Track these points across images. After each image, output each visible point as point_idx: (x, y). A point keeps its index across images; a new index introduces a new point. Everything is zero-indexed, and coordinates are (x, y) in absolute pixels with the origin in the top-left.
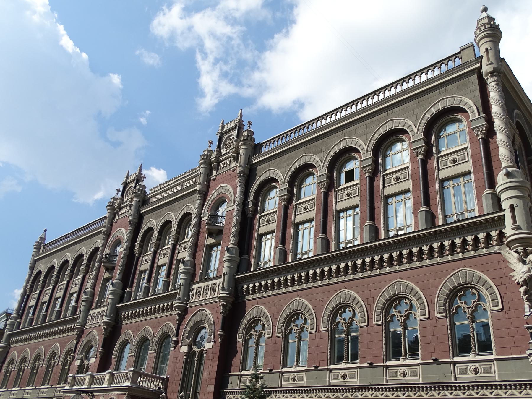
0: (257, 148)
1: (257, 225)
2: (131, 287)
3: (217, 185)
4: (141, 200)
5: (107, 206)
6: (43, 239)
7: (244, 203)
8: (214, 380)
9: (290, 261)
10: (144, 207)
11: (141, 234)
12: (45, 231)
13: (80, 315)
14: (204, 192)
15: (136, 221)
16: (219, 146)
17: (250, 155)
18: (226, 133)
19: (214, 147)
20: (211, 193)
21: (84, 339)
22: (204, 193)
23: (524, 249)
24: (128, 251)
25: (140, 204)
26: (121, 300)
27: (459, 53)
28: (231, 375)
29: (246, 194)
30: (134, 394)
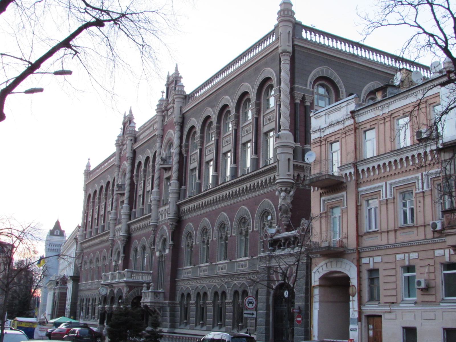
0: (186, 98)
2: (135, 208)
4: (133, 139)
6: (88, 166)
7: (180, 146)
8: (170, 274)
9: (229, 179)
11: (136, 167)
12: (89, 159)
13: (111, 231)
16: (167, 96)
17: (181, 107)
18: (170, 84)
19: (165, 97)
21: (115, 248)
23: (281, 188)
25: (133, 142)
26: (130, 220)
27: (274, 30)
29: (181, 138)
30: (130, 285)
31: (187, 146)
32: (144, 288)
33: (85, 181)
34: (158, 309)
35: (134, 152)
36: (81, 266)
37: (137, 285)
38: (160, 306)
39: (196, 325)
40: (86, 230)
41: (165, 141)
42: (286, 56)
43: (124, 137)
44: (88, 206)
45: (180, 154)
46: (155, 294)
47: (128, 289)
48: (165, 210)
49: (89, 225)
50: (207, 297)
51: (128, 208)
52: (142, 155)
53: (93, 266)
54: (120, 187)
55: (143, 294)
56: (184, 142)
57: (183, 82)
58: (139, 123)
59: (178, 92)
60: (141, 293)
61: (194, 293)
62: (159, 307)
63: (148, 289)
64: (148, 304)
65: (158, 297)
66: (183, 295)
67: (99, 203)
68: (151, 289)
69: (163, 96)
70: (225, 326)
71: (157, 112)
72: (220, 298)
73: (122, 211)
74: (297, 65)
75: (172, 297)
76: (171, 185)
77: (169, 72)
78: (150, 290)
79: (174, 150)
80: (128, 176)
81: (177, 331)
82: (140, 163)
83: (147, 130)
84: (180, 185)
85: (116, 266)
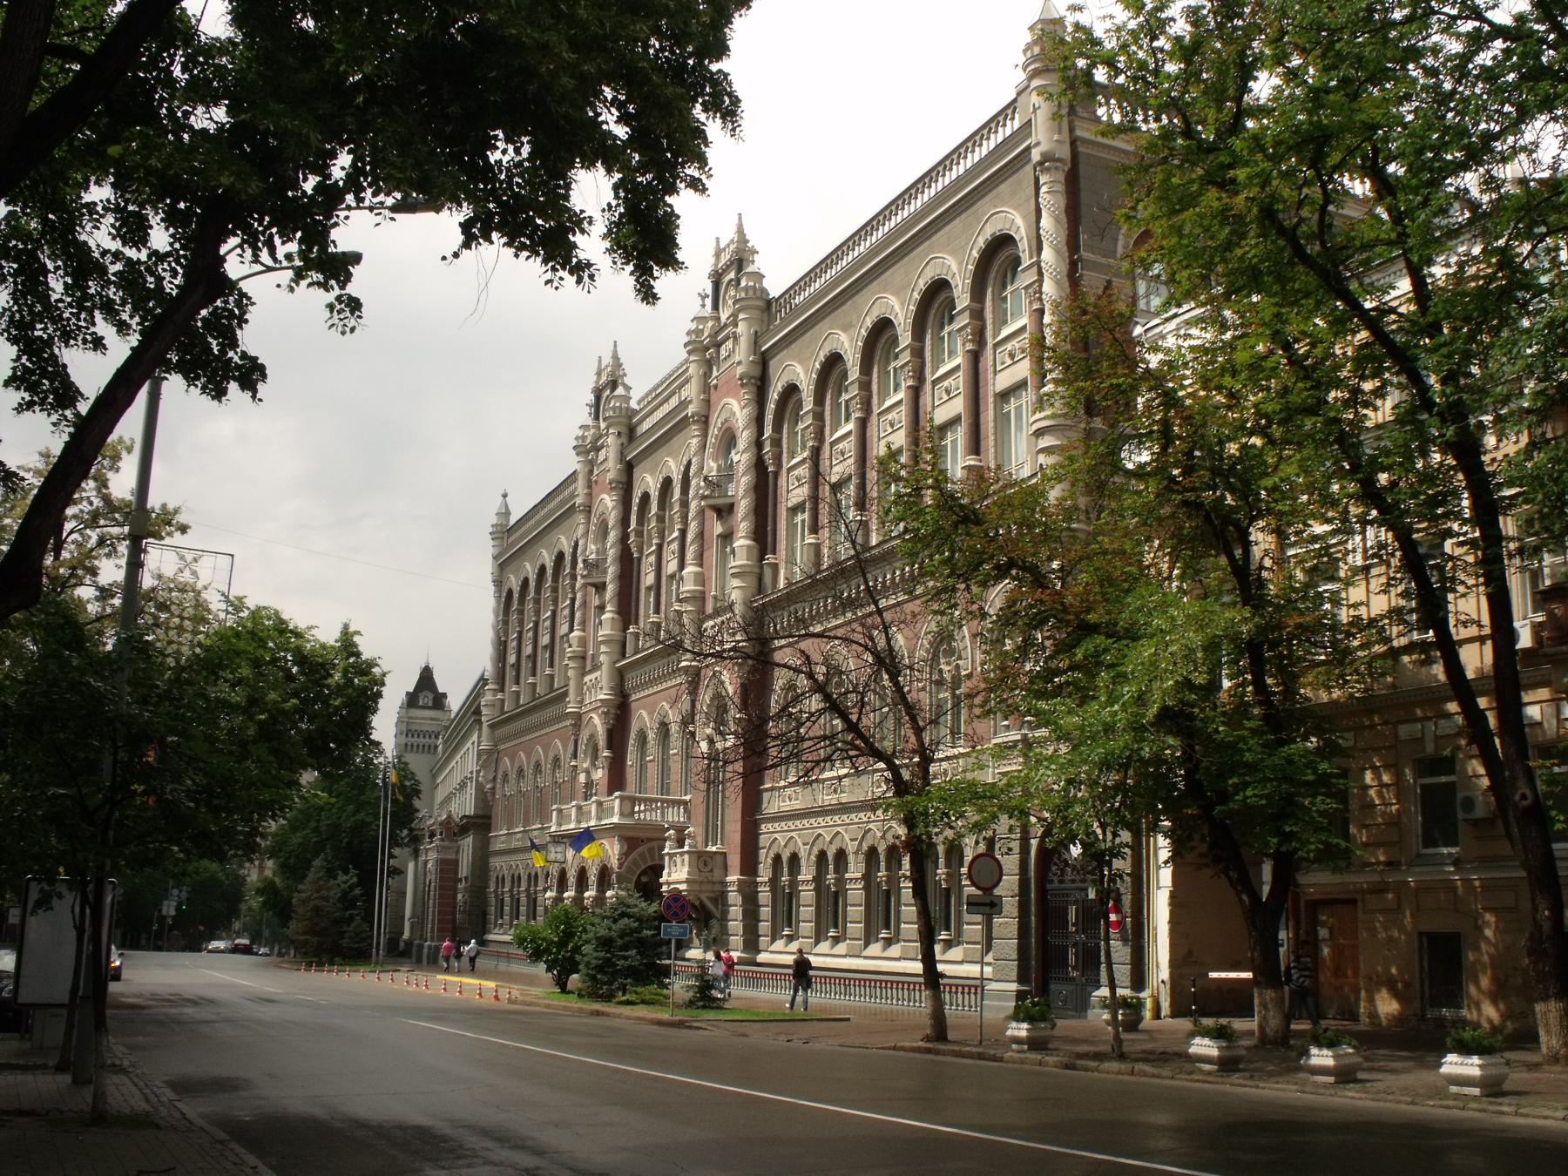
0: (767, 307)
1: (785, 488)
3: (720, 399)
4: (624, 430)
5: (574, 448)
7: (759, 444)
10: (632, 446)
11: (635, 508)
12: (505, 496)
15: (624, 479)
16: (716, 307)
18: (724, 271)
20: (713, 421)
21: (584, 736)
24: (620, 547)
25: (624, 439)
26: (623, 656)
27: (1015, 101)
28: (767, 790)
29: (759, 421)
30: (631, 834)
31: (777, 443)
32: (668, 844)
33: (495, 558)
34: (710, 899)
35: (629, 468)
36: (493, 788)
37: (648, 835)
39: (817, 943)
40: (502, 690)
41: (714, 431)
42: (1053, 171)
43: (599, 428)
44: (506, 623)
45: (759, 465)
46: (699, 857)
47: (625, 848)
48: (723, 622)
49: (510, 673)
52: (651, 475)
53: (526, 786)
54: (594, 566)
55: (667, 858)
56: (768, 432)
57: (760, 263)
58: (639, 385)
59: (747, 294)
60: (662, 857)
61: (809, 854)
62: (712, 895)
63: (681, 844)
64: (683, 887)
65: (709, 868)
66: (777, 859)
67: (538, 613)
68: (690, 846)
69: (703, 306)
70: (898, 941)
71: (690, 353)
73: (600, 633)
74: (1085, 196)
75: (749, 864)
77: (718, 239)
78: (686, 848)
79: (741, 457)
80: (613, 536)
81: (762, 957)
82: (646, 497)
83: (661, 404)
85: (589, 784)
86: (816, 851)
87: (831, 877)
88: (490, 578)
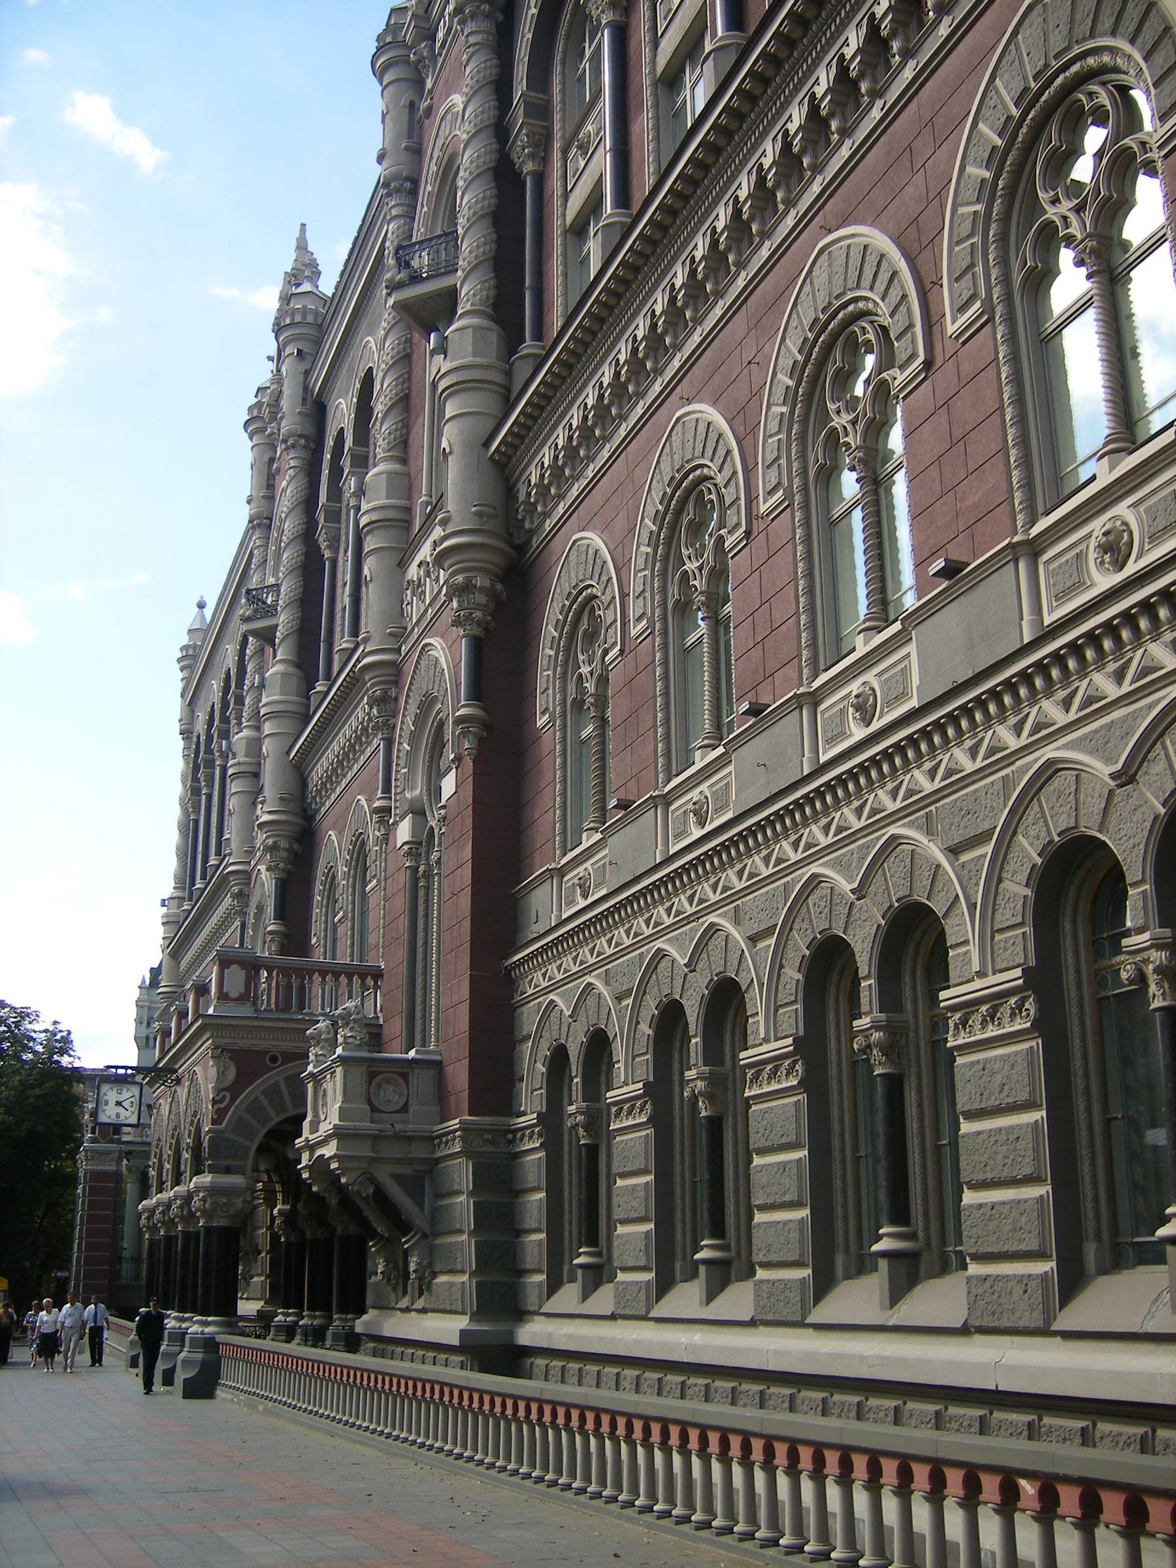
14: (407, 179)
15: (310, 430)
22: (408, 185)
29: (501, 86)
30: (243, 1043)
31: (541, 111)
34: (398, 1178)
38: (410, 1162)
39: (664, 1285)
46: (372, 1076)
47: (232, 1074)
50: (742, 1018)
51: (294, 682)
62: (407, 1170)
65: (397, 1101)
66: (559, 1056)
72: (868, 985)
73: (264, 700)
76: (452, 346)
81: (531, 1333)
84: (512, 338)
86: (650, 1008)
87: (695, 1076)
88: (177, 727)
